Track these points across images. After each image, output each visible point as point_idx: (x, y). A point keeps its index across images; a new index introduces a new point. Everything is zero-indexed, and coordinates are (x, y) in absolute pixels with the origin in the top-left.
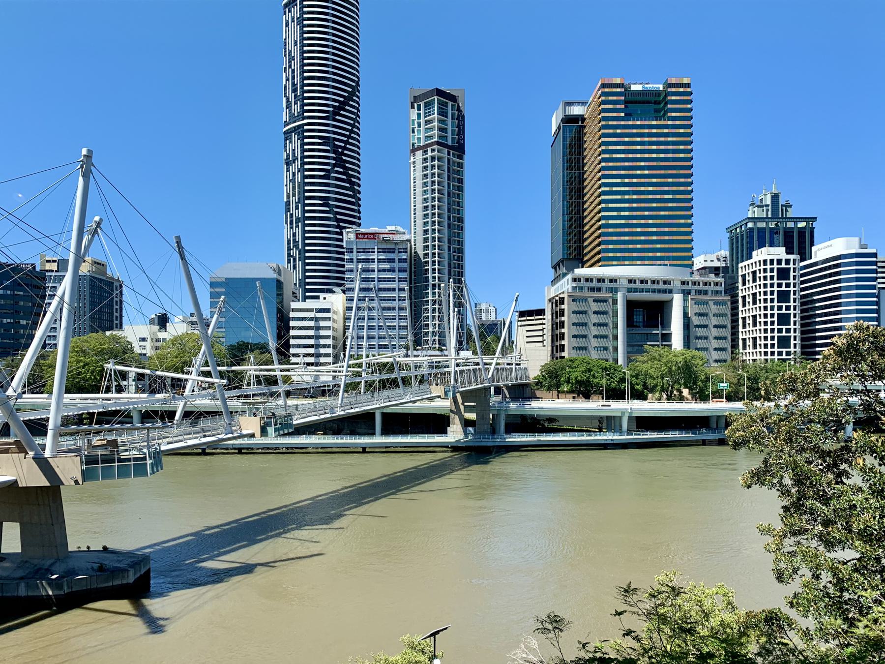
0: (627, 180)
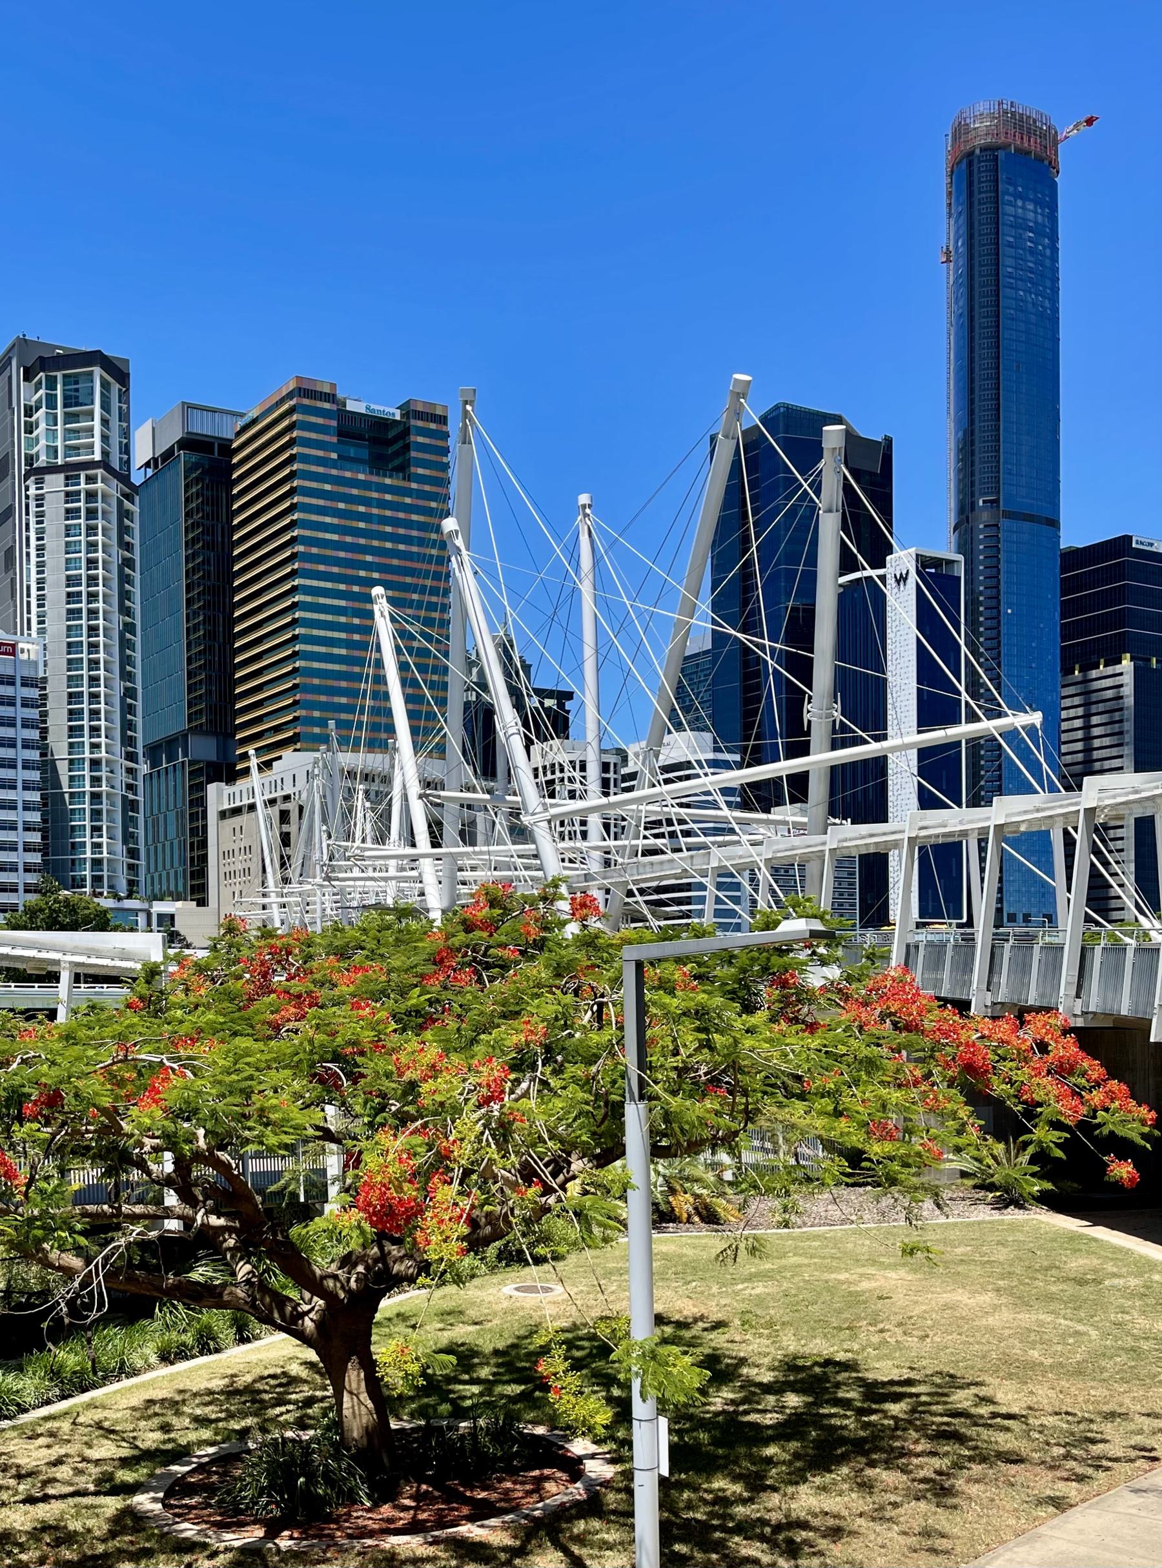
0: (342, 587)
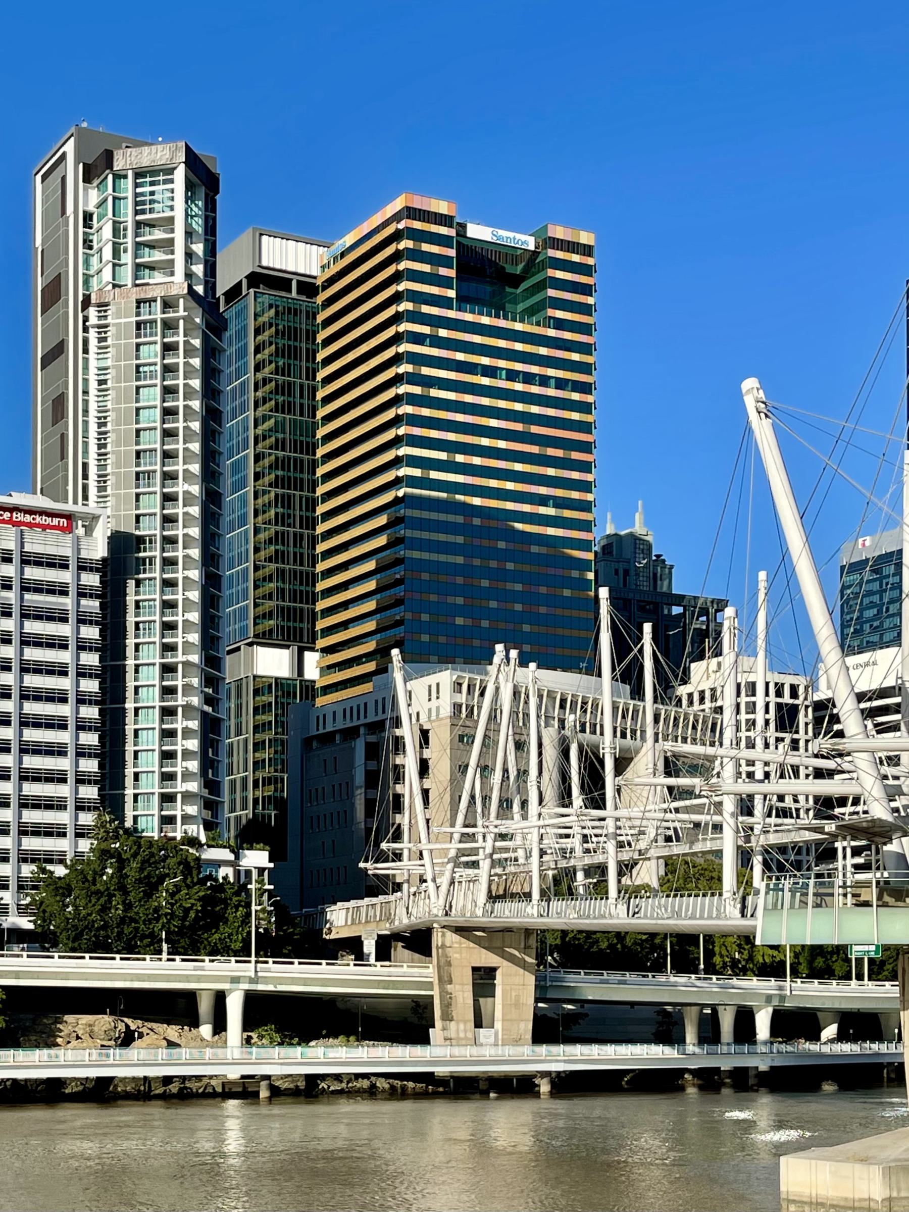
0: (460, 458)
